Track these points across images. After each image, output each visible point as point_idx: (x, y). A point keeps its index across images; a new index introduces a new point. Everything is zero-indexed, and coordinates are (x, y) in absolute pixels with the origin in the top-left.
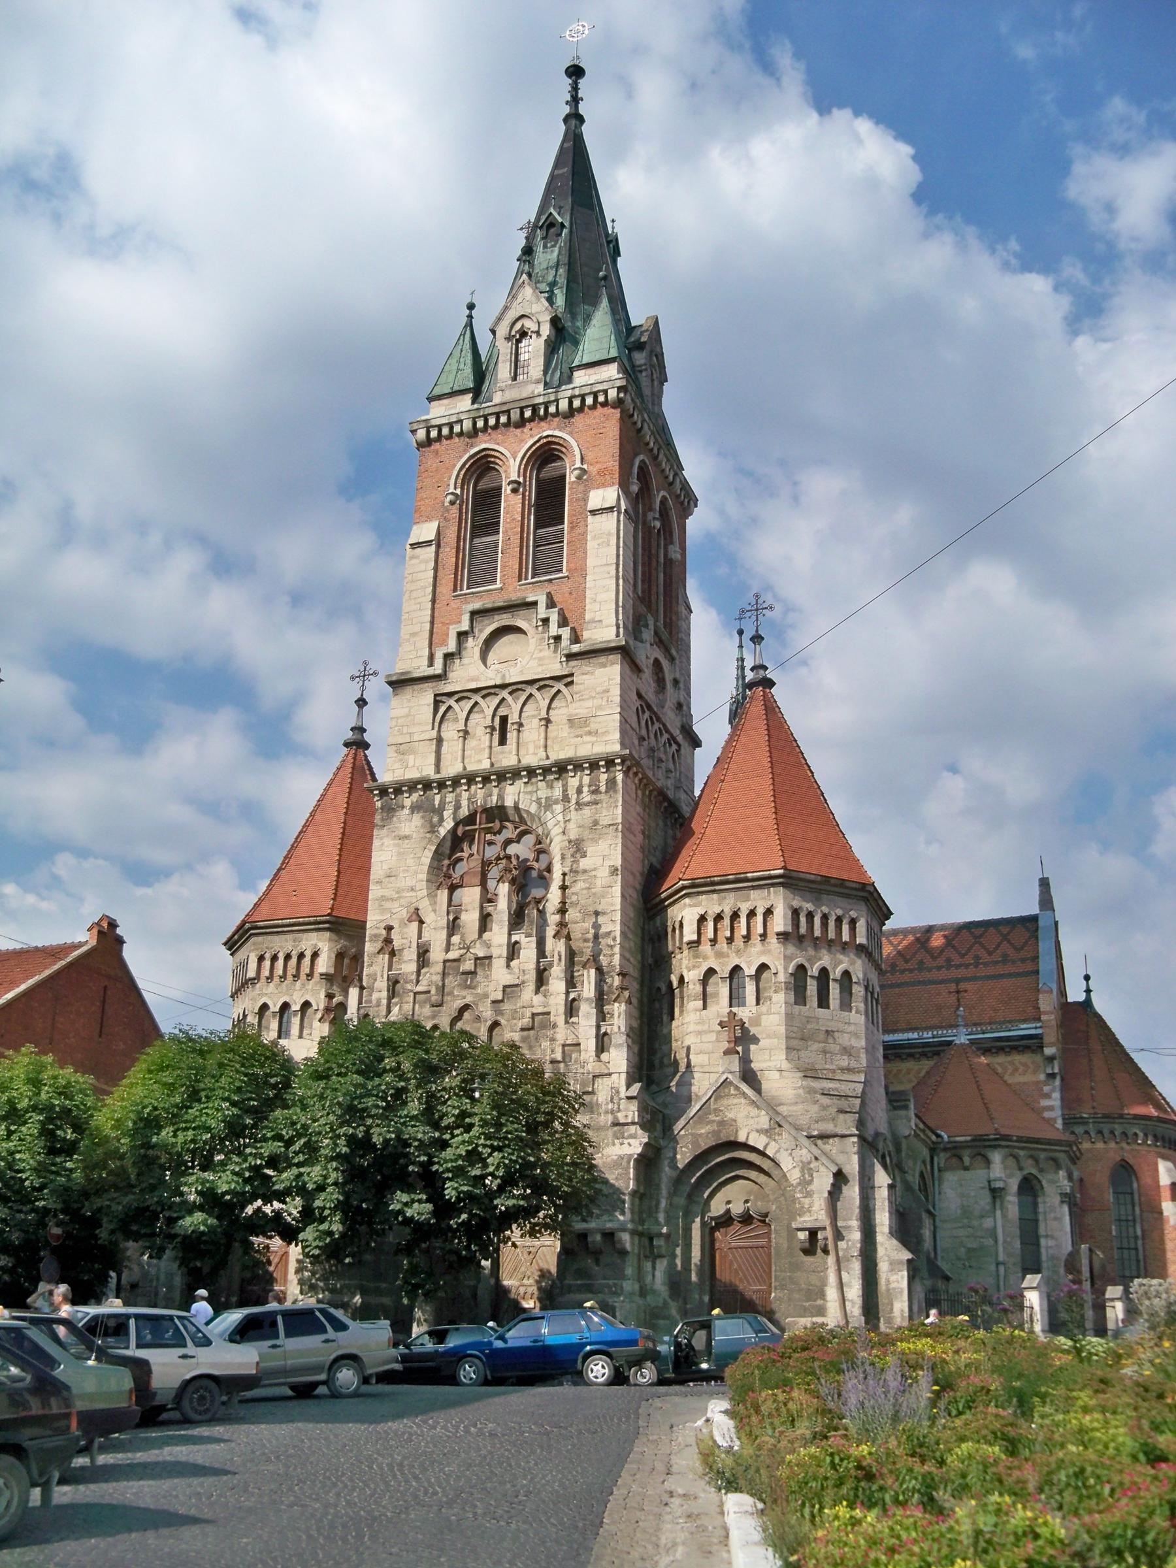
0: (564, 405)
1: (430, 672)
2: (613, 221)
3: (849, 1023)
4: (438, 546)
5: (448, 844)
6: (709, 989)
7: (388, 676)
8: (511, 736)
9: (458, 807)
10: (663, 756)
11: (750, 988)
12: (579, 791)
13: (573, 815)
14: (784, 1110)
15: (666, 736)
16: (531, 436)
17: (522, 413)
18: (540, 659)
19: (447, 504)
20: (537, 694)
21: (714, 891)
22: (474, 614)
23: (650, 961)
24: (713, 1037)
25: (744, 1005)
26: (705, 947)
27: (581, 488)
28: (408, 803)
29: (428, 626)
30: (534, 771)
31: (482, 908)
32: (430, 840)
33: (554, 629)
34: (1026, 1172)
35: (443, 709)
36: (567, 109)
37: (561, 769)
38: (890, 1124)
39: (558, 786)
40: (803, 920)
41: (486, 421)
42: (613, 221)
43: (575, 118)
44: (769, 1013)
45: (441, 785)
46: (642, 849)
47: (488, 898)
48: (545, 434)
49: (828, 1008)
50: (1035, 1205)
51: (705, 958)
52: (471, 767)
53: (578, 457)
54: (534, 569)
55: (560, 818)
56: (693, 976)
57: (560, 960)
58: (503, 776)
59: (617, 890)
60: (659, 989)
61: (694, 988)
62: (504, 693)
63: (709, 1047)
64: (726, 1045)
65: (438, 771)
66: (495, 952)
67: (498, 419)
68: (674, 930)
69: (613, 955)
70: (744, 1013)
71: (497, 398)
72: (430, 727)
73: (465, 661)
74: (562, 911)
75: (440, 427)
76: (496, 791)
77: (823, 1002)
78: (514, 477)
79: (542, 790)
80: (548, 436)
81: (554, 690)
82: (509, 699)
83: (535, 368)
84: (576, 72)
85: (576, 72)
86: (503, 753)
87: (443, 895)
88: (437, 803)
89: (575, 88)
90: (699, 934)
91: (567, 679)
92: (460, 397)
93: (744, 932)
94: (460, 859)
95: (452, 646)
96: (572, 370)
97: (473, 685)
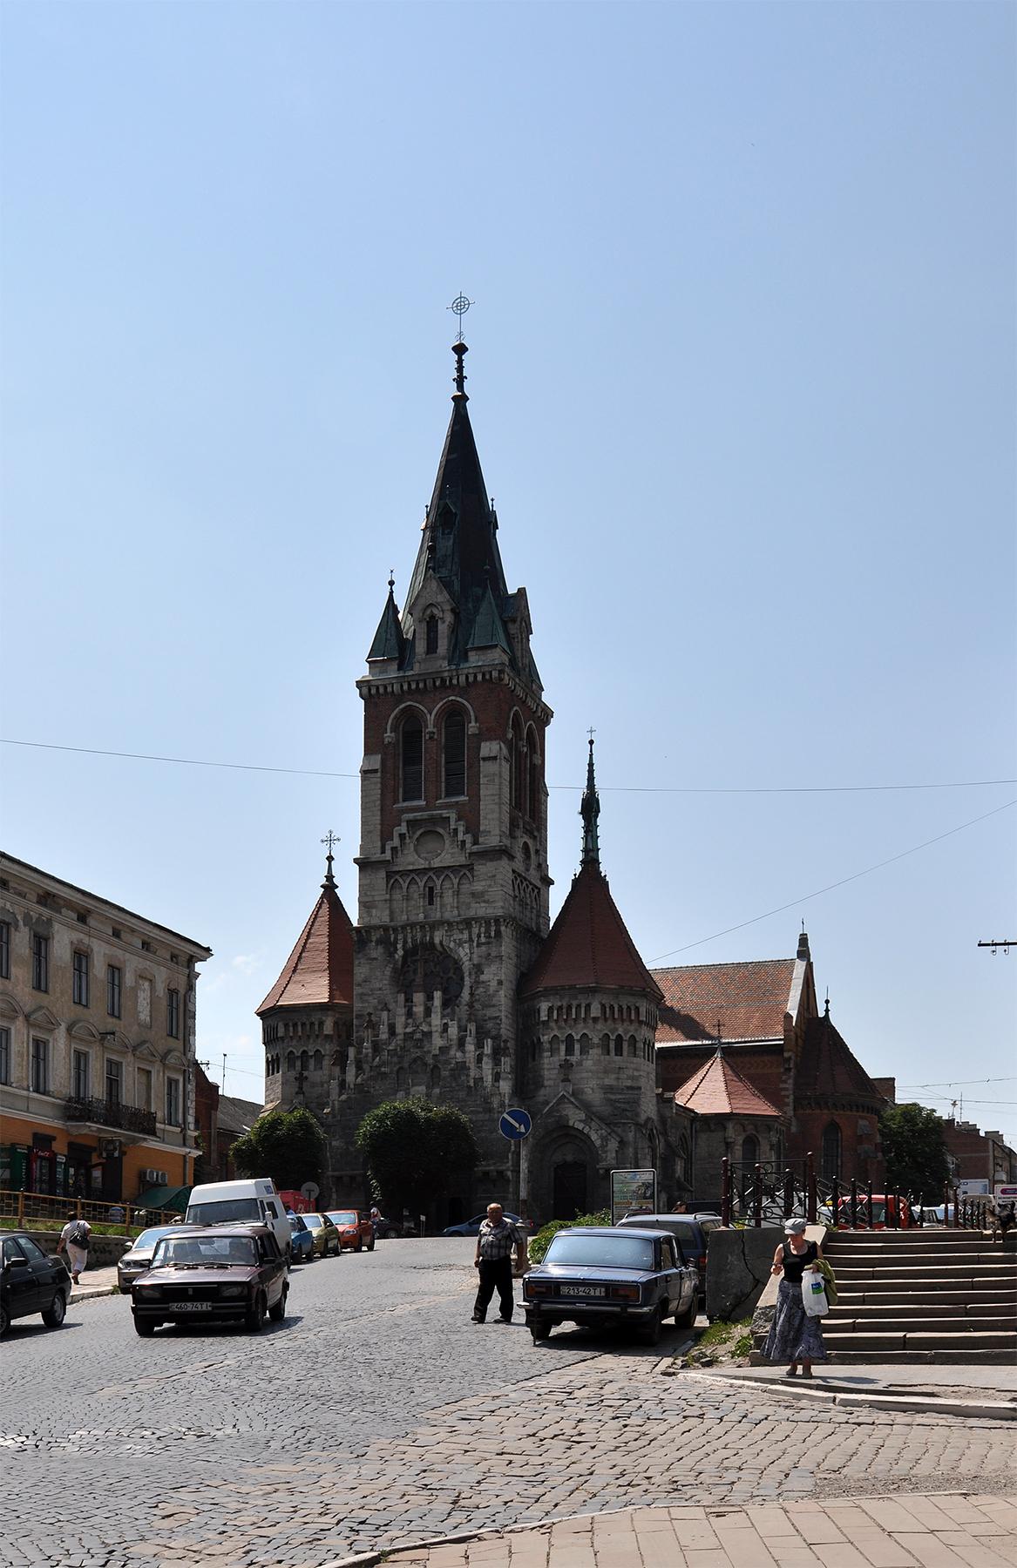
0: (462, 679)
3: (633, 1063)
4: (382, 772)
5: (400, 963)
6: (555, 1046)
8: (437, 900)
9: (405, 942)
10: (528, 902)
11: (577, 1046)
12: (479, 936)
13: (476, 949)
14: (594, 1109)
15: (531, 887)
16: (442, 699)
17: (434, 682)
18: (452, 854)
19: (386, 740)
20: (452, 876)
21: (557, 994)
22: (408, 822)
23: (521, 1027)
24: (556, 1071)
25: (573, 1055)
26: (553, 1024)
28: (374, 939)
29: (379, 827)
30: (452, 924)
31: (426, 1005)
32: (389, 962)
34: (748, 1133)
37: (468, 923)
38: (659, 1111)
39: (466, 932)
40: (608, 1009)
41: (409, 685)
44: (587, 1059)
45: (395, 930)
46: (516, 966)
47: (430, 998)
48: (450, 698)
49: (621, 1055)
50: (755, 1150)
51: (552, 1030)
52: (413, 919)
54: (446, 791)
55: (468, 951)
56: (545, 1039)
57: (471, 1033)
58: (434, 926)
59: (502, 993)
60: (526, 1043)
61: (547, 1046)
62: (431, 874)
63: (554, 1076)
64: (562, 1077)
65: (391, 920)
66: (434, 1029)
67: (418, 684)
68: (535, 1012)
69: (500, 1029)
70: (573, 1059)
71: (417, 669)
72: (384, 892)
73: (405, 852)
74: (471, 1005)
76: (428, 934)
77: (619, 1052)
78: (431, 728)
79: (457, 936)
80: (452, 700)
81: (462, 873)
82: (434, 878)
83: (443, 646)
86: (432, 909)
87: (401, 997)
88: (392, 939)
90: (548, 1016)
91: (470, 868)
92: (393, 663)
93: (574, 1017)
94: (408, 971)
95: (396, 842)
97: (411, 868)
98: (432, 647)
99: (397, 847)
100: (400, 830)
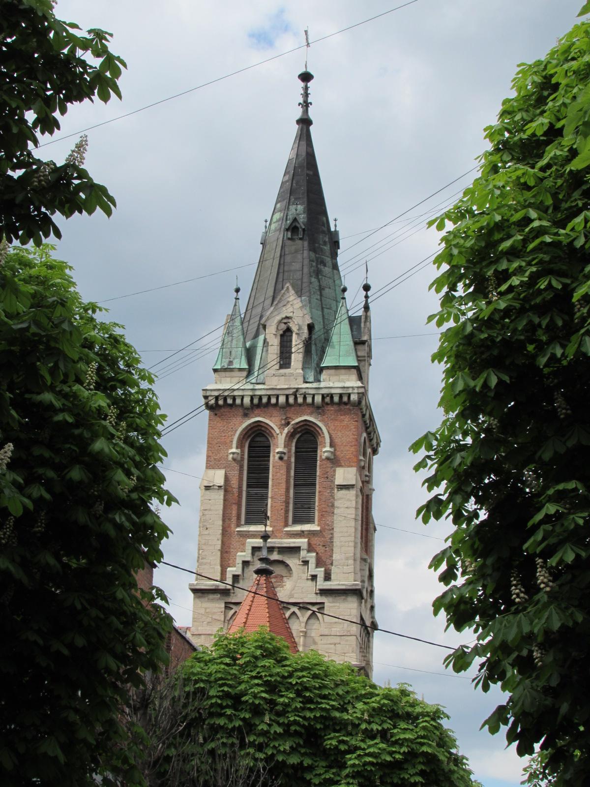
0: (318, 399)
1: (222, 586)
2: (335, 220)
7: (190, 585)
27: (329, 464)
33: (312, 569)
35: (232, 612)
36: (298, 113)
42: (335, 220)
43: (305, 122)
53: (328, 440)
75: (225, 399)
78: (280, 449)
80: (306, 420)
84: (306, 77)
85: (306, 77)
89: (306, 95)
96: (322, 369)
98: (285, 360)
99: (238, 576)
100: (244, 556)
